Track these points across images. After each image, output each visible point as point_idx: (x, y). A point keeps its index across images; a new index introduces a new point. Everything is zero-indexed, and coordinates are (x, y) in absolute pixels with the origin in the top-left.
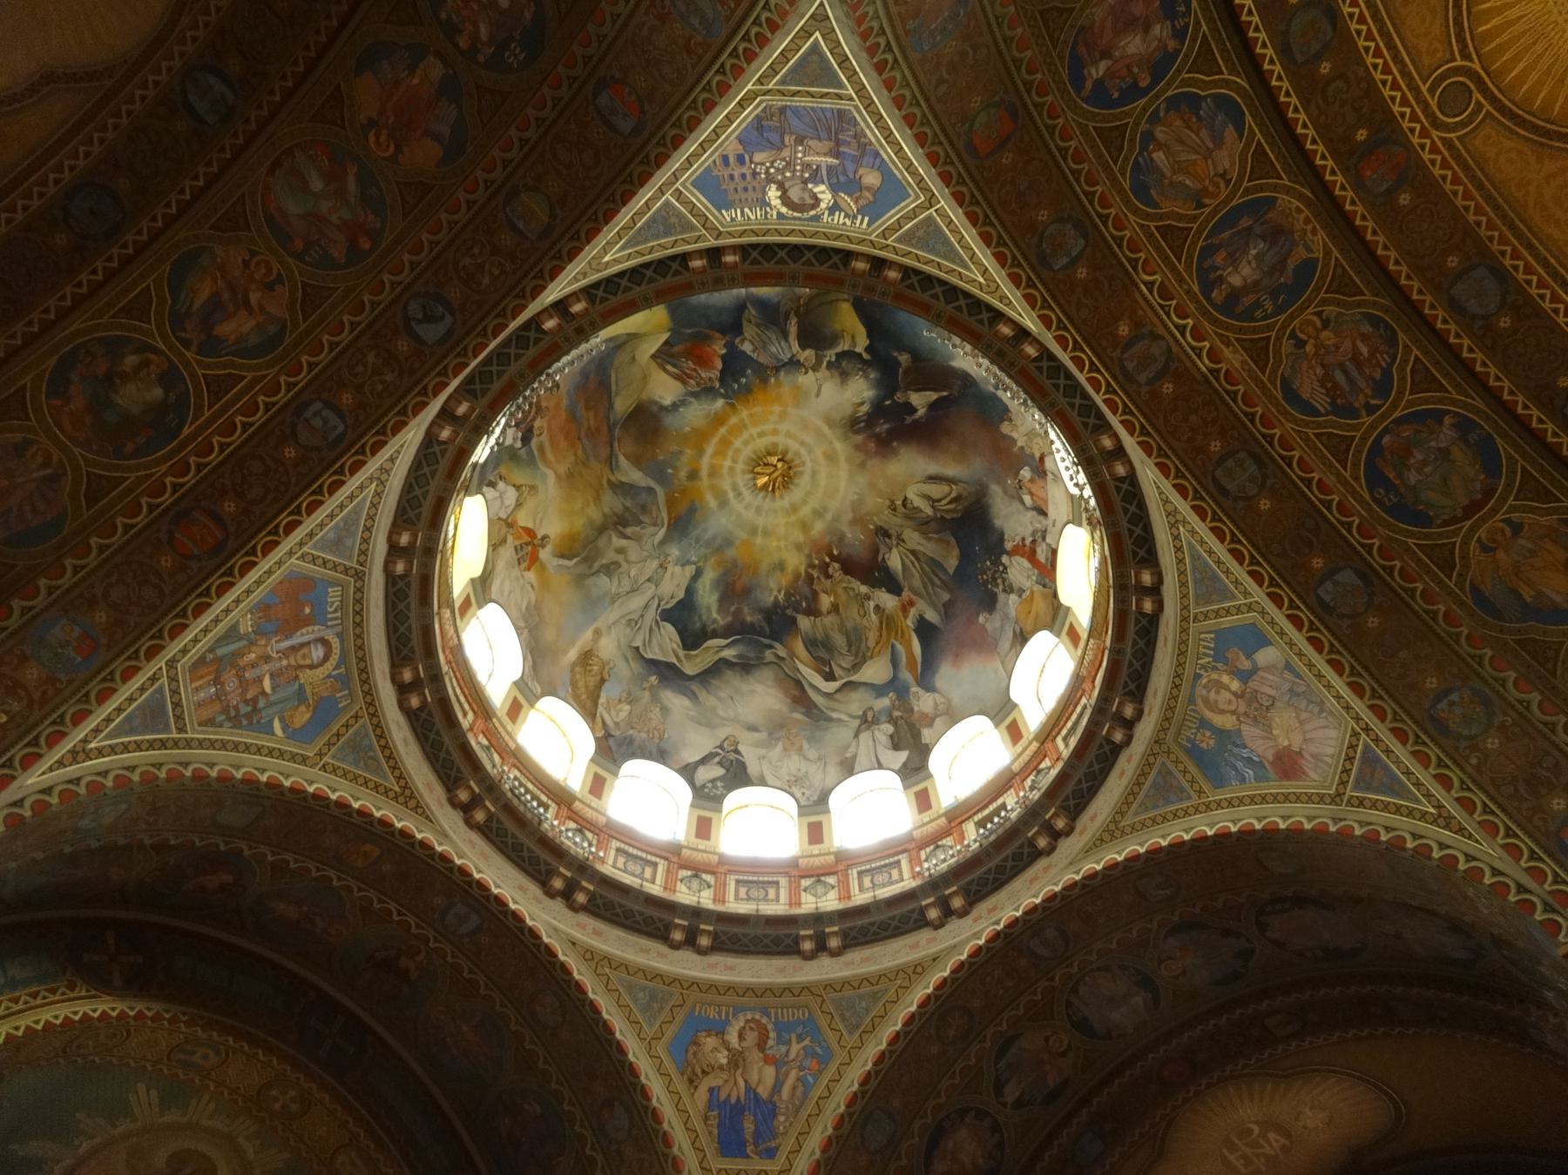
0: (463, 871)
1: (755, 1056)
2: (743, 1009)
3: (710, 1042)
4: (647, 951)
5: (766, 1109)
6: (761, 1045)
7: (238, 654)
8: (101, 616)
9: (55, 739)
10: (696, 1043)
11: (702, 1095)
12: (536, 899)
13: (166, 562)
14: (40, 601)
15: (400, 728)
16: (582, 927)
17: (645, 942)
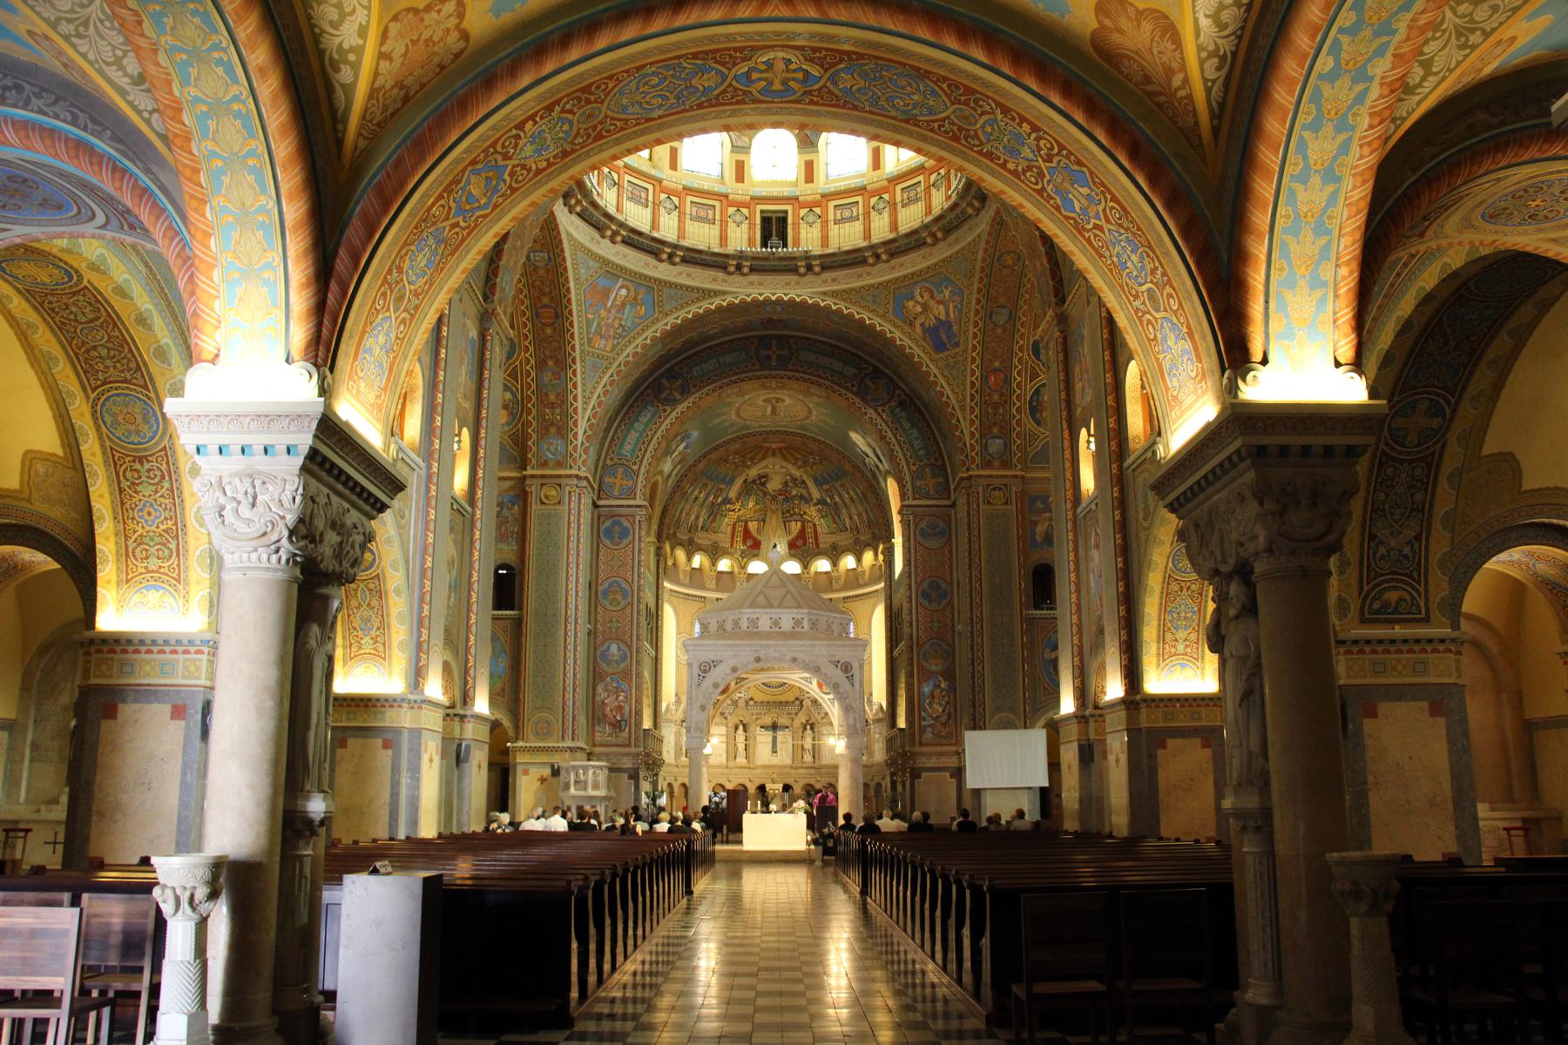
0: (755, 301)
1: (932, 303)
2: (916, 283)
3: (910, 304)
4: (859, 276)
5: (947, 324)
6: (932, 297)
7: (598, 324)
8: (551, 363)
9: (575, 410)
10: (904, 307)
11: (918, 329)
12: (797, 283)
13: (549, 331)
14: (533, 374)
15: (680, 274)
16: (825, 282)
17: (859, 270)
